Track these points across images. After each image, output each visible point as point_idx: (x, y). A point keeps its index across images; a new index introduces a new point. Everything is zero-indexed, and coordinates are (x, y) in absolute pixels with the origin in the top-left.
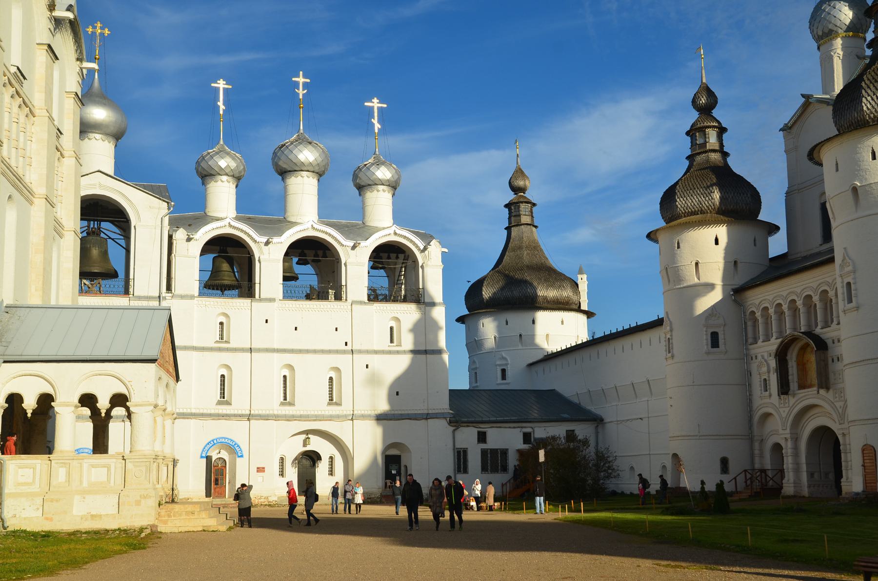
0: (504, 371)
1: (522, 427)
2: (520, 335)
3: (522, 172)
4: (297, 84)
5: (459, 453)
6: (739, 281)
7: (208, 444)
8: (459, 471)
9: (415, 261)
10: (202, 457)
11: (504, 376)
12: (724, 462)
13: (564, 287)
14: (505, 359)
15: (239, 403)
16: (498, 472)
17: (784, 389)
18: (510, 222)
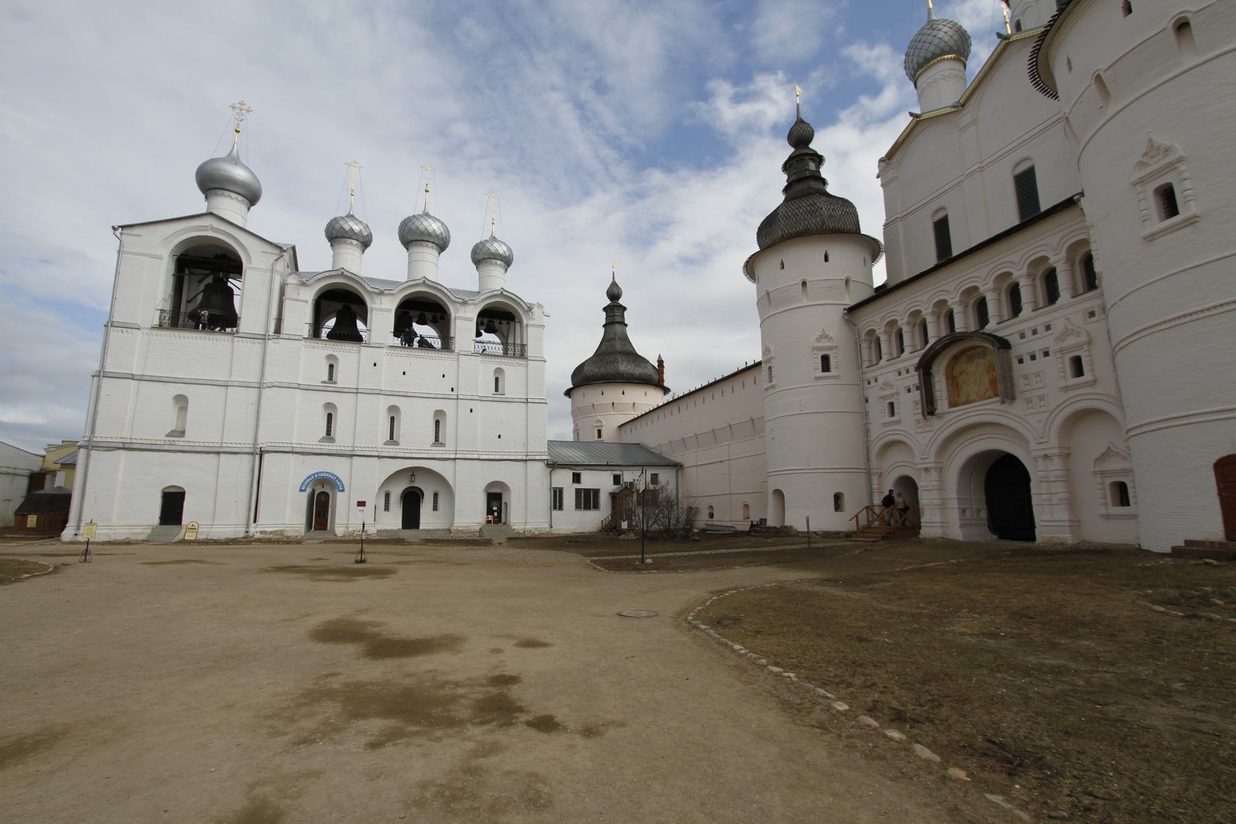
0: (599, 431)
1: (612, 470)
2: (613, 404)
5: (555, 492)
6: (851, 301)
7: (308, 478)
8: (555, 508)
10: (301, 490)
11: (600, 436)
12: (838, 498)
14: (601, 422)
15: (343, 437)
16: (590, 509)
17: (929, 407)
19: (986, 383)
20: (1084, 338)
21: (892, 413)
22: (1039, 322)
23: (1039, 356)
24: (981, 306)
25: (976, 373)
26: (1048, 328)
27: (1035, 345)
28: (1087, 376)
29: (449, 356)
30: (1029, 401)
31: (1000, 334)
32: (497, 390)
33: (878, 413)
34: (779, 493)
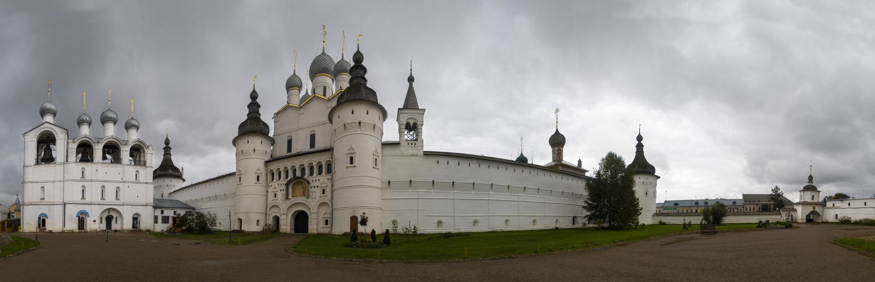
12: (258, 221)
17: (287, 198)
19: (301, 192)
20: (326, 185)
21: (275, 197)
22: (317, 178)
23: (316, 187)
24: (303, 170)
25: (299, 190)
26: (319, 180)
27: (315, 184)
28: (325, 195)
30: (312, 198)
31: (307, 179)
33: (271, 197)
34: (240, 220)
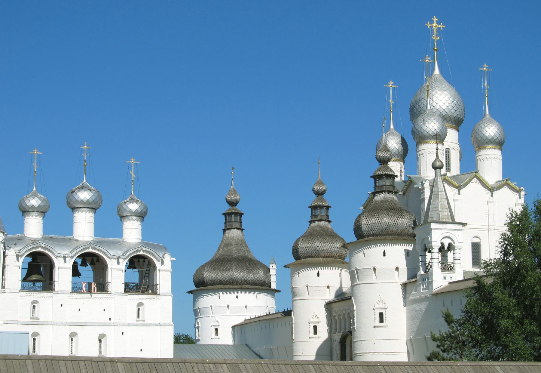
2: (228, 306)
3: (235, 191)
4: (82, 150)
9: (155, 267)
13: (259, 273)
14: (217, 321)
18: (225, 226)
29: (108, 296)
32: (138, 317)
